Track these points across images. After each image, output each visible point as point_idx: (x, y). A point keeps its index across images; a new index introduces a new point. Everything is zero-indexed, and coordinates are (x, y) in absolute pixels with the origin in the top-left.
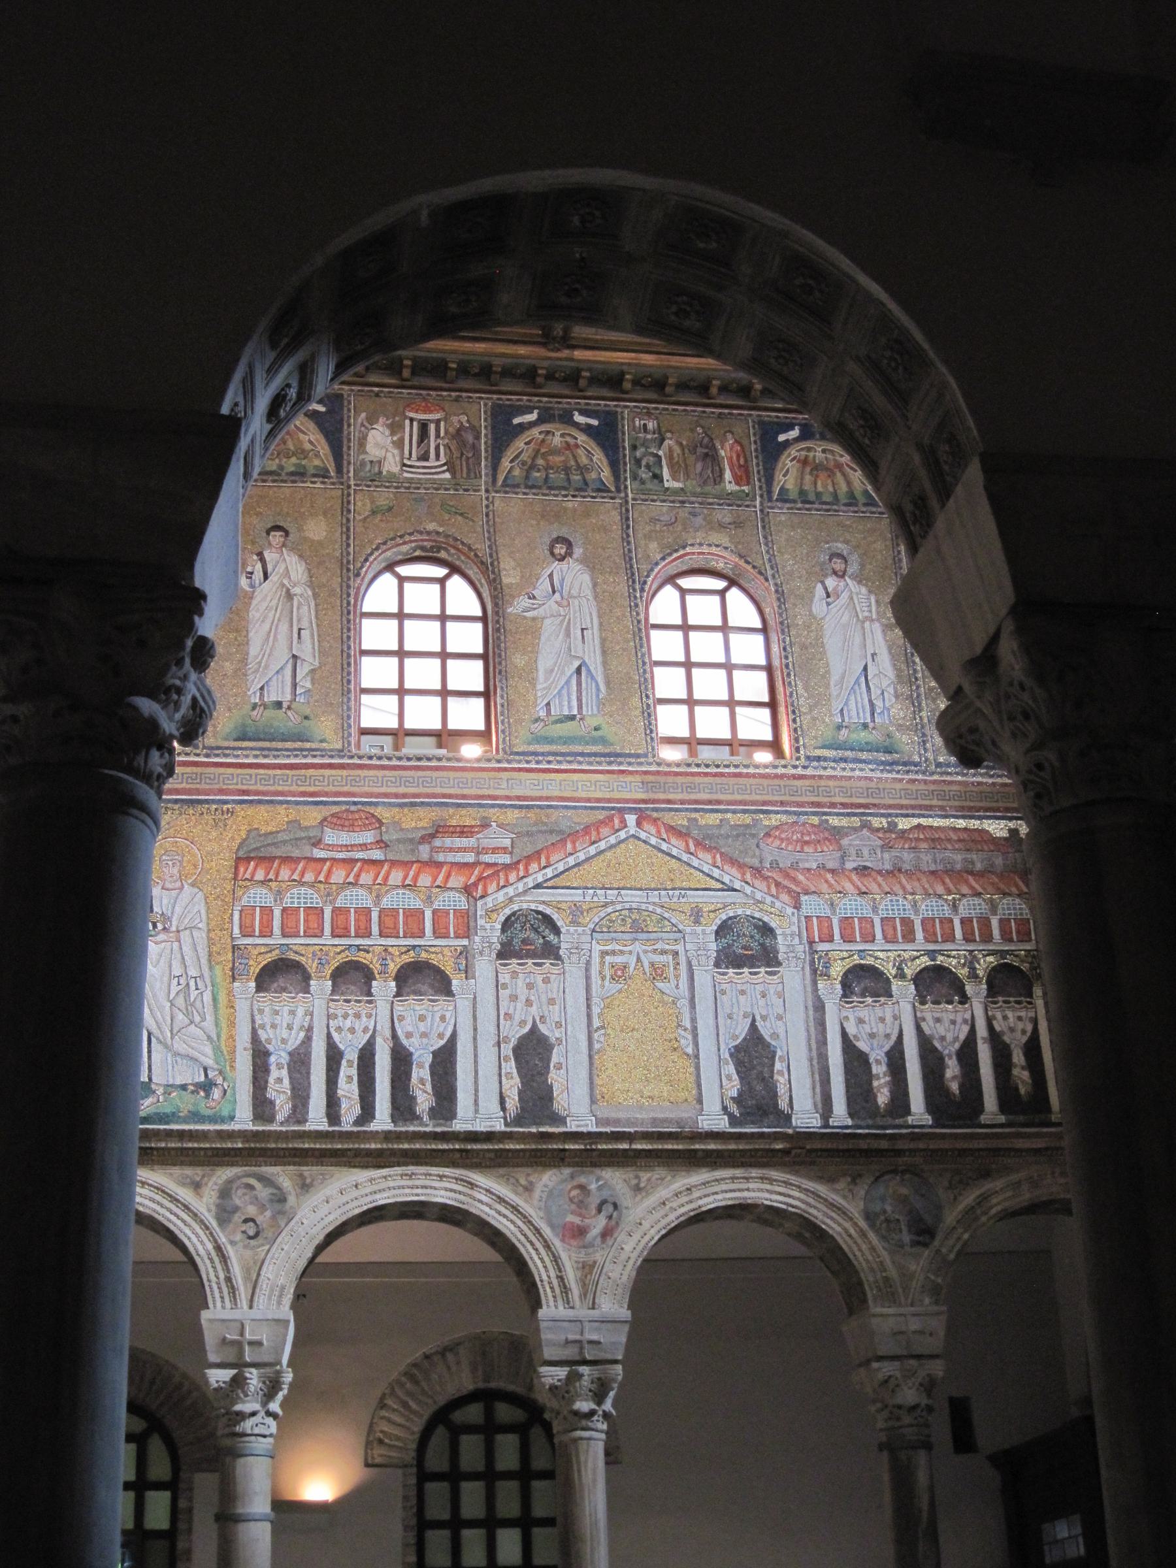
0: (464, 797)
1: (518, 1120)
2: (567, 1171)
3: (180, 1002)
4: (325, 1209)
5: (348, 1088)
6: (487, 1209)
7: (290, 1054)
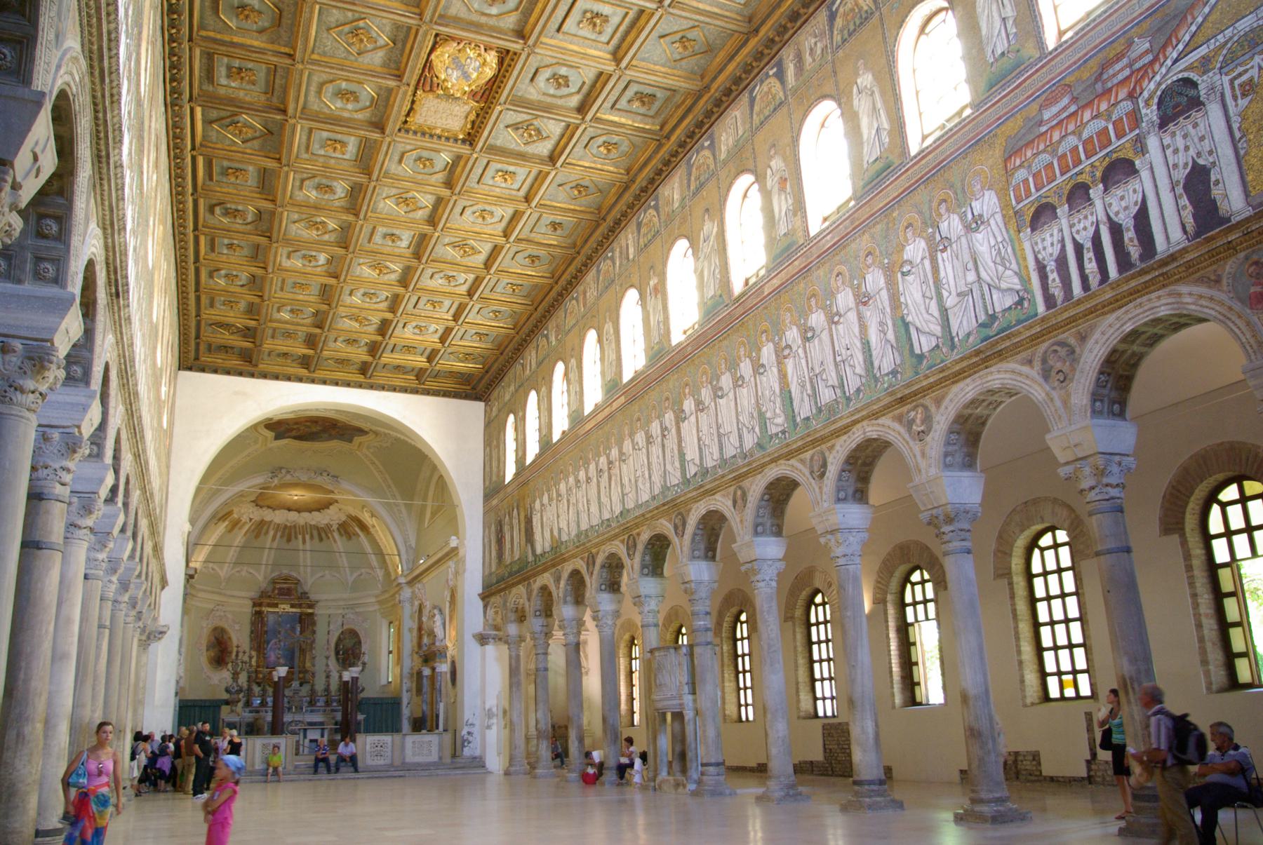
0: (1113, 34)
1: (1198, 234)
2: (1242, 255)
3: (998, 260)
4: (1098, 347)
5: (1091, 266)
6: (1193, 307)
7: (1056, 261)
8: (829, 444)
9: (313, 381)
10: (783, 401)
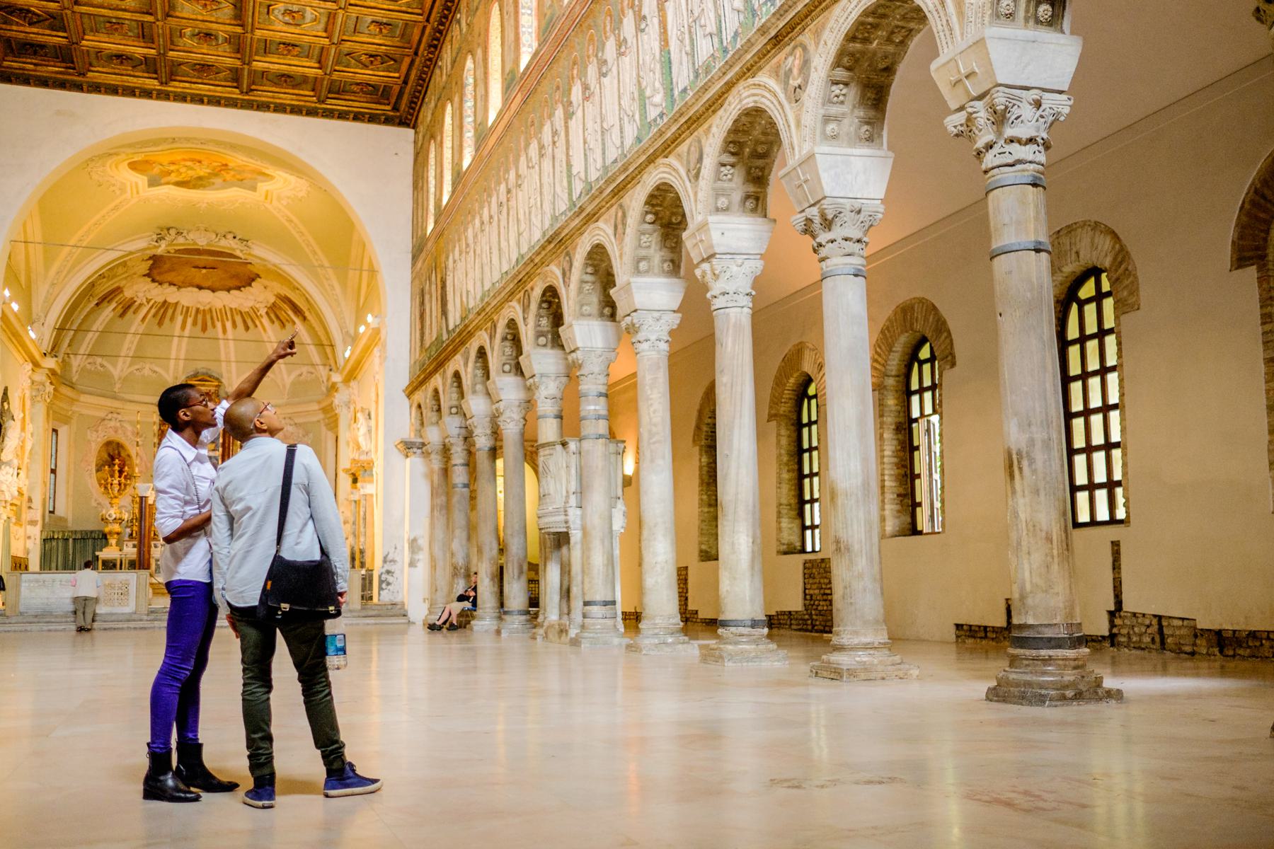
8: (706, 126)
9: (165, 96)
10: (662, 68)
